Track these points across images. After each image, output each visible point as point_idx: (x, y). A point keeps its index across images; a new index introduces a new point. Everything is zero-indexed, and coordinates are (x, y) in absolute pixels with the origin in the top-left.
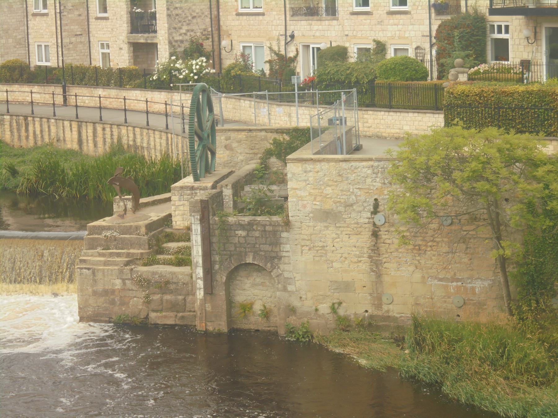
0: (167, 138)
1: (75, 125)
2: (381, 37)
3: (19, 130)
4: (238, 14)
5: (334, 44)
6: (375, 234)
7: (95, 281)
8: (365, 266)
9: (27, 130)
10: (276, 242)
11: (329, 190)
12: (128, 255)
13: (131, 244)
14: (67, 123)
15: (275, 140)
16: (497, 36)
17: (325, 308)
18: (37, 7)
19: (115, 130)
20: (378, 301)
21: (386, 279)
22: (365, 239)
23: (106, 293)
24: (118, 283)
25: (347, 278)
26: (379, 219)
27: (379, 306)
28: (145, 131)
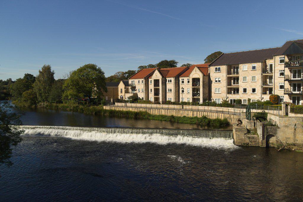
0: (218, 114)
1: (192, 112)
2: (250, 98)
3: (177, 113)
4: (215, 93)
5: (238, 99)
6: (295, 130)
7: (239, 137)
8: (293, 135)
9: (179, 113)
10: (276, 130)
11: (286, 122)
12: (244, 133)
13: (244, 131)
14: (190, 112)
15: (255, 114)
16: (281, 98)
17: (284, 142)
18: (169, 91)
19: (202, 113)
20: (295, 141)
21: (296, 137)
22: (293, 130)
23: (241, 139)
24: (244, 138)
25: (289, 137)
26: (296, 127)
27: (295, 141)
28: (211, 113)
